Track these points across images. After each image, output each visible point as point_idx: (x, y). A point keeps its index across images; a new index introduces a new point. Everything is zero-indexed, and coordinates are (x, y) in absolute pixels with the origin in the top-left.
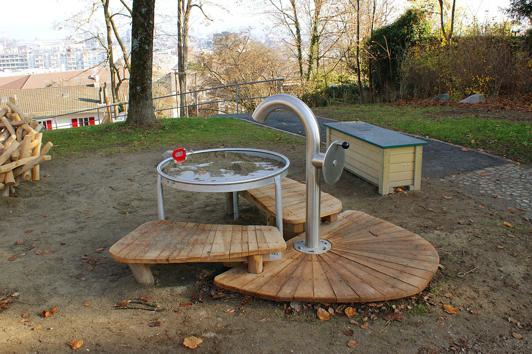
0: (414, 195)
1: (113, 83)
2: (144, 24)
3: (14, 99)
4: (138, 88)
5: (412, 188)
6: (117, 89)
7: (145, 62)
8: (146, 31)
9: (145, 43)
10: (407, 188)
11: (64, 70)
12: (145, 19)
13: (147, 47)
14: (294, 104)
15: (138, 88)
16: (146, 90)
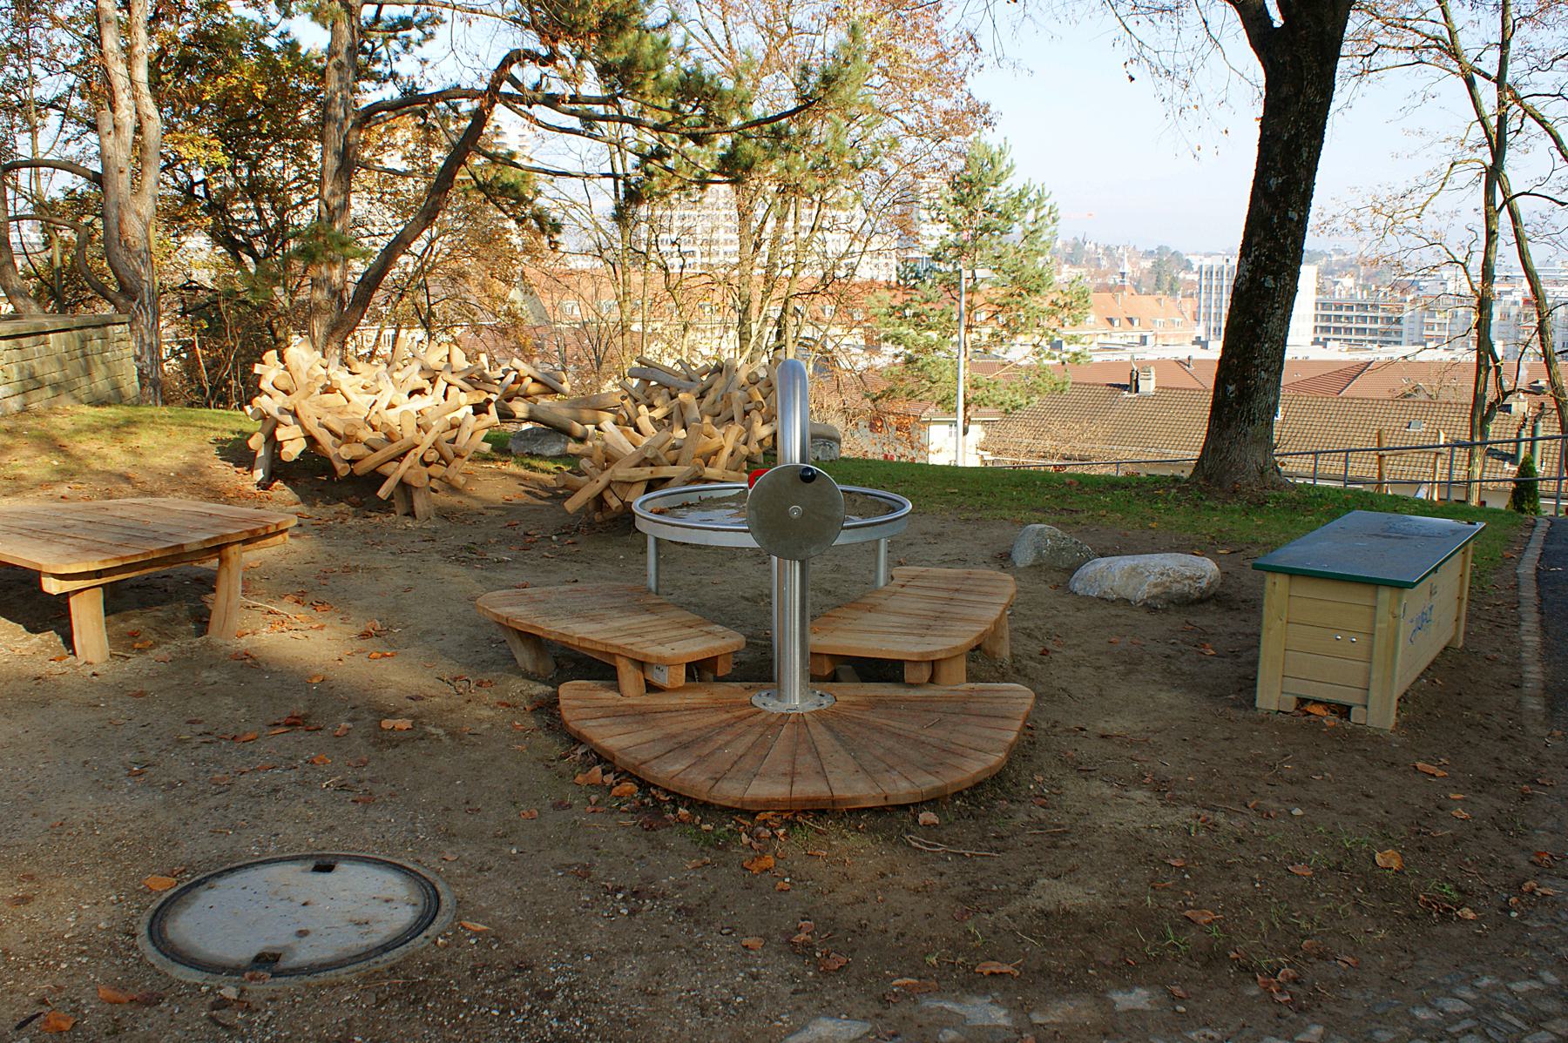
0: (1355, 737)
1: (1478, 398)
2: (1271, 219)
3: (815, 368)
4: (1231, 388)
5: (1357, 716)
6: (1486, 419)
7: (1259, 322)
8: (1275, 238)
9: (1265, 271)
10: (1344, 711)
11: (363, 269)
12: (1276, 207)
13: (1270, 282)
14: (782, 387)
15: (1231, 388)
16: (1250, 397)
